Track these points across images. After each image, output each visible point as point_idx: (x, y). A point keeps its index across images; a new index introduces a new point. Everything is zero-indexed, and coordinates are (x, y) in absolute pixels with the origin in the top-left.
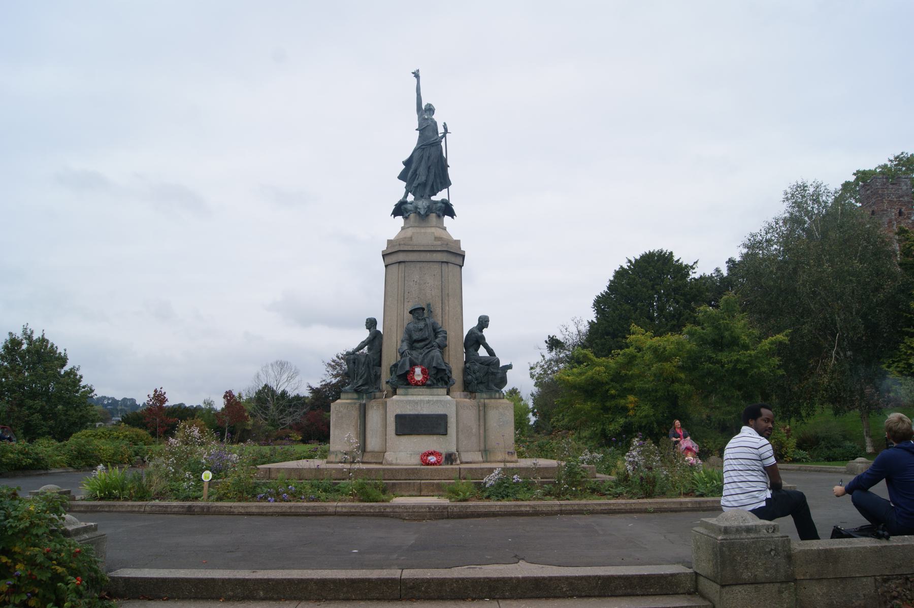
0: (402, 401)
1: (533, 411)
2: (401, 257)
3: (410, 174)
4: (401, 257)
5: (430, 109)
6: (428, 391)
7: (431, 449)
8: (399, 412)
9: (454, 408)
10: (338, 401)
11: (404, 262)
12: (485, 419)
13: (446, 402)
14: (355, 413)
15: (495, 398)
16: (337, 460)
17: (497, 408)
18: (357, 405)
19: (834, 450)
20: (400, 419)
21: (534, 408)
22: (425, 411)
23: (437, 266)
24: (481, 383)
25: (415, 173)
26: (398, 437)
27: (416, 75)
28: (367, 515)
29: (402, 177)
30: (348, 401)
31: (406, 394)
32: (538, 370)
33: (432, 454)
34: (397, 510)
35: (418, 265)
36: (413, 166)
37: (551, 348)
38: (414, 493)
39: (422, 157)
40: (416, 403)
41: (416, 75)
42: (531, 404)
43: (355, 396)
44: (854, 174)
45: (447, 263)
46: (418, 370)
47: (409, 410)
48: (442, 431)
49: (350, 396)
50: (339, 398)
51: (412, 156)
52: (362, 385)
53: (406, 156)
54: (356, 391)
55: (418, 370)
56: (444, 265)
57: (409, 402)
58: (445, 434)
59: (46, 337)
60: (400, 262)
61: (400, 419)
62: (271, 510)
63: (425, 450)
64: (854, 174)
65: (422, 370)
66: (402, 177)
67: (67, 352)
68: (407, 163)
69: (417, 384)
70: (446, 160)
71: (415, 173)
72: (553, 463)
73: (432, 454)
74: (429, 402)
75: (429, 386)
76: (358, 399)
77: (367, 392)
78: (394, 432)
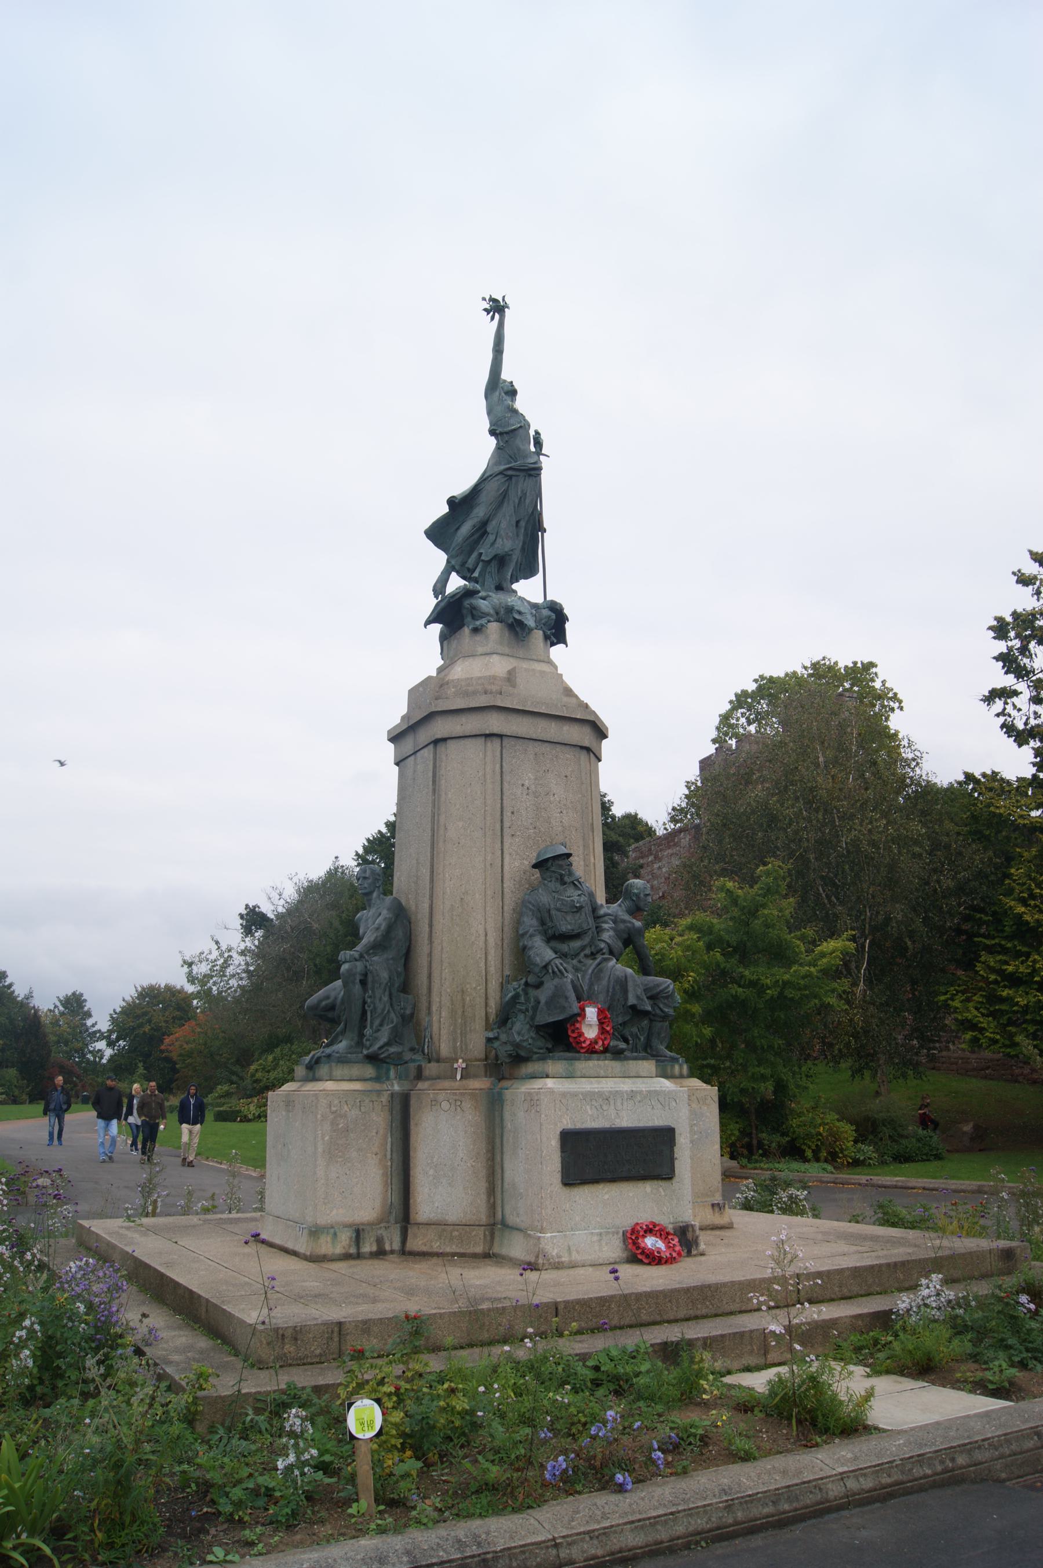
0: (575, 1095)
1: (108, 1038)
2: (495, 723)
3: (466, 529)
4: (495, 723)
6: (615, 1066)
7: (645, 1217)
8: (568, 1124)
9: (684, 1112)
11: (501, 736)
13: (670, 1096)
14: (379, 1119)
16: (339, 1250)
18: (385, 1098)
19: (904, 1141)
20: (572, 1141)
21: (110, 1032)
22: (627, 1118)
23: (569, 754)
25: (481, 530)
26: (566, 1191)
27: (497, 308)
28: (921, 1489)
29: (438, 533)
30: (357, 1086)
31: (570, 1076)
32: (202, 969)
33: (651, 1229)
34: (978, 1456)
35: (532, 747)
36: (480, 512)
37: (248, 931)
38: (752, 1361)
39: (504, 497)
40: (606, 1098)
41: (497, 308)
42: (104, 1026)
43: (370, 1071)
44: (756, 681)
46: (591, 1013)
47: (591, 1120)
49: (356, 1070)
51: (475, 492)
52: (388, 1044)
53: (461, 486)
54: (372, 1059)
55: (591, 1013)
57: (590, 1097)
60: (488, 736)
61: (572, 1141)
62: (680, 1529)
63: (628, 1224)
64: (756, 681)
65: (600, 1012)
66: (438, 533)
68: (459, 506)
69: (591, 1051)
71: (481, 530)
72: (984, 1244)
74: (632, 1095)
75: (617, 1054)
76: (377, 1079)
77: (398, 1061)
78: (557, 1177)
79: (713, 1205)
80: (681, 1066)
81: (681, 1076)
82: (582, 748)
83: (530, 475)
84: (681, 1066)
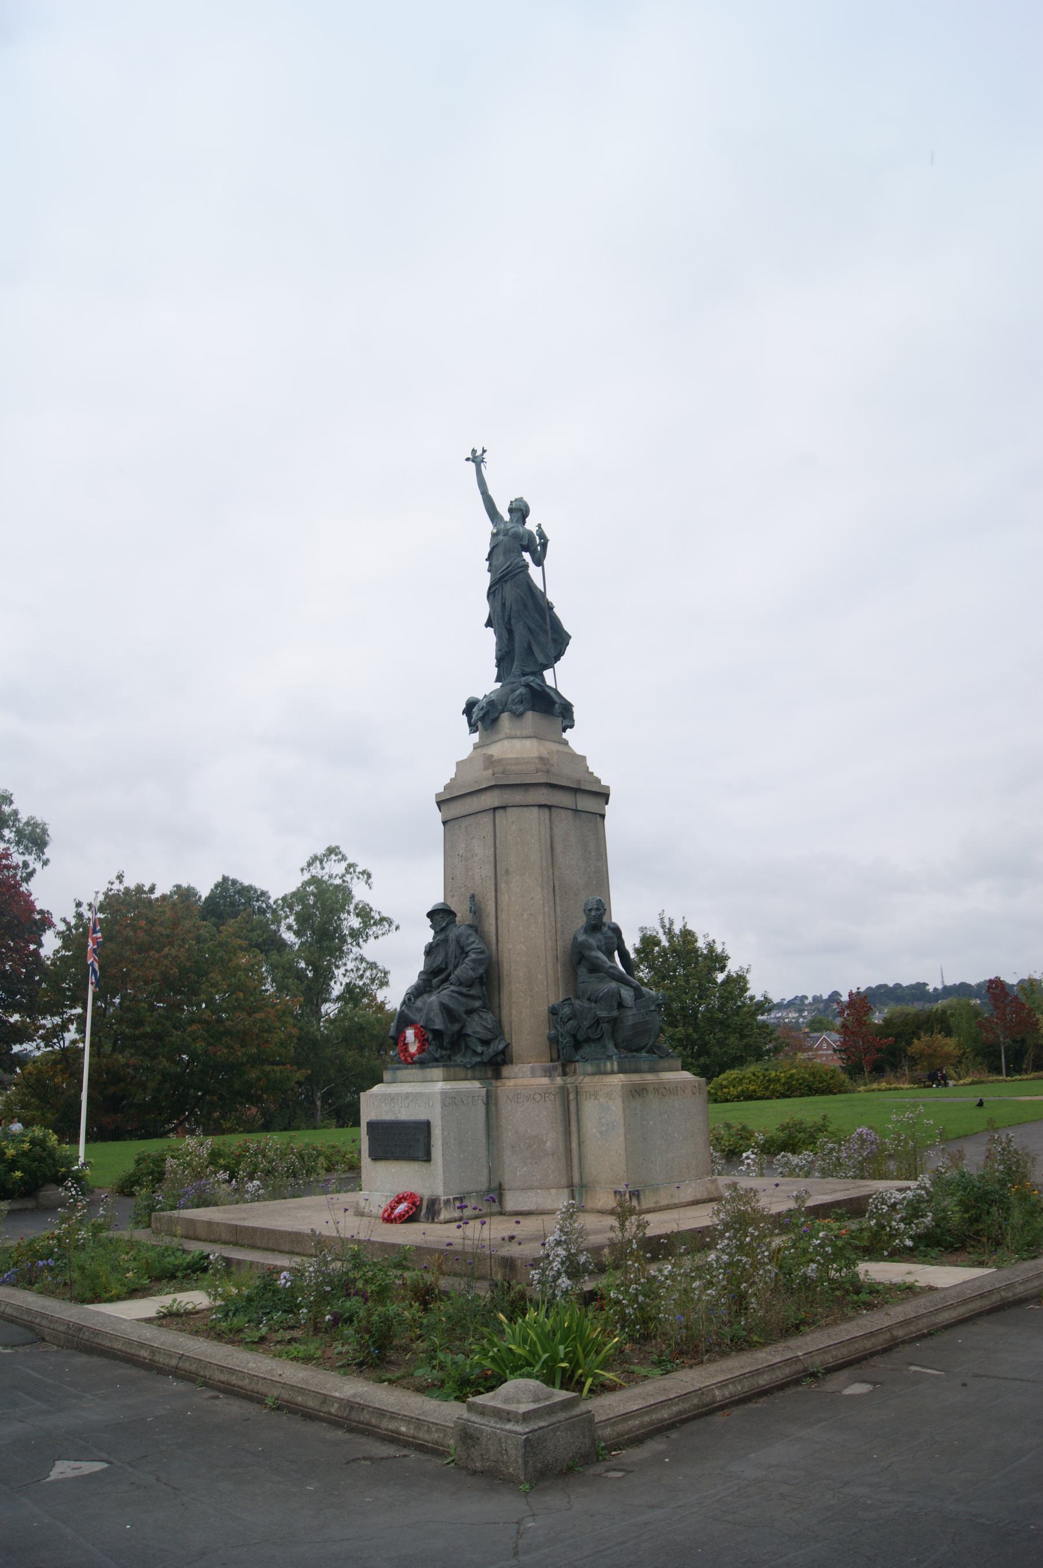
5: (520, 511)
10: (377, 1089)
12: (578, 1120)
15: (606, 1073)
17: (596, 1095)
22: (405, 1114)
23: (486, 819)
24: (588, 1040)
40: (391, 1098)
41: (477, 460)
45: (504, 808)
46: (410, 1033)
48: (421, 1154)
50: (380, 1081)
56: (499, 814)
58: (428, 1159)
59: (689, 927)
67: (726, 947)
70: (544, 594)
73: (399, 1200)
79: (615, 1192)
80: (612, 1064)
81: (613, 1073)
82: (495, 809)
83: (506, 581)
84: (612, 1064)
